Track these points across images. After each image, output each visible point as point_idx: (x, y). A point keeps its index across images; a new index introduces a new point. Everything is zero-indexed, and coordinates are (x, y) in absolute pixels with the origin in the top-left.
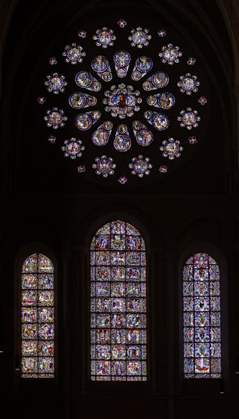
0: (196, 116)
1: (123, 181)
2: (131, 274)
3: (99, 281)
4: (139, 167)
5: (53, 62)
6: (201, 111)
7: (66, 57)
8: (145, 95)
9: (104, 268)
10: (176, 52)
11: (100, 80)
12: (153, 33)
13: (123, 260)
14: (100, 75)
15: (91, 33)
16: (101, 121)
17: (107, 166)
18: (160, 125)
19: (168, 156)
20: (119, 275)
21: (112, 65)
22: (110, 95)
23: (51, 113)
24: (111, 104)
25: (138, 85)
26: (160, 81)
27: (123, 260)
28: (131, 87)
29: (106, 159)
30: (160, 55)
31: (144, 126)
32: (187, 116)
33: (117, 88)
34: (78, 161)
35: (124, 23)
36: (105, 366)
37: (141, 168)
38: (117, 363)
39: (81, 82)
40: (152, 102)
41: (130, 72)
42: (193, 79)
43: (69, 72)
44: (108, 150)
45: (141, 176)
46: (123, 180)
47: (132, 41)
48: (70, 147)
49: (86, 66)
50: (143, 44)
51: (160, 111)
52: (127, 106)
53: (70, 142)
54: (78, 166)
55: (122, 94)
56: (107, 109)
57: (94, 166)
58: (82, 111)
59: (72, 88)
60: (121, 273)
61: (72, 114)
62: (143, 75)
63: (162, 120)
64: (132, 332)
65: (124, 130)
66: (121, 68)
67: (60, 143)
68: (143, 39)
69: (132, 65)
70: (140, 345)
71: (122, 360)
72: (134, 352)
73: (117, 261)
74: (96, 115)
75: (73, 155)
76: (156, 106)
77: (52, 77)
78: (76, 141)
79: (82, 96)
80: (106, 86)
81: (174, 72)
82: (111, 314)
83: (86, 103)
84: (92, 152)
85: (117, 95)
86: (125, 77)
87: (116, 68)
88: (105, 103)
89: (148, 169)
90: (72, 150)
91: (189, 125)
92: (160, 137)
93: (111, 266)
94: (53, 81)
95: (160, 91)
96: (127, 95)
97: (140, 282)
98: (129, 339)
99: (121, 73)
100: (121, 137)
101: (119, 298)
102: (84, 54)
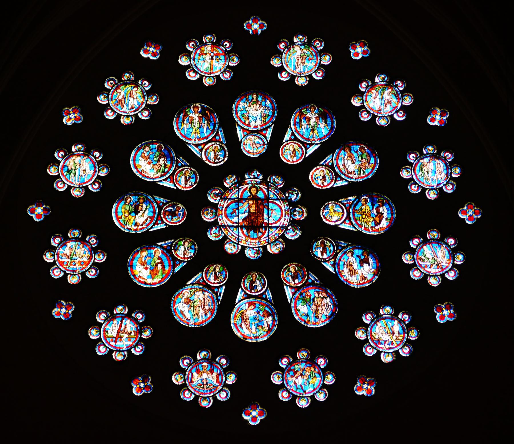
0: (453, 252)
1: (254, 419)
4: (300, 381)
5: (70, 119)
6: (465, 240)
7: (107, 107)
8: (315, 199)
10: (397, 96)
11: (196, 162)
12: (337, 48)
14: (195, 150)
15: (174, 48)
16: (194, 267)
17: (212, 378)
18: (356, 273)
19: (379, 353)
21: (228, 125)
22: (224, 199)
23: (63, 244)
24: (223, 220)
25: (296, 176)
26: (354, 165)
28: (279, 180)
29: (211, 361)
30: (356, 102)
31: (313, 277)
32: (427, 250)
33: (241, 182)
34: (132, 366)
35: (261, 26)
37: (304, 383)
39: (146, 164)
40: (333, 215)
41: (276, 142)
42: (444, 160)
43: (113, 142)
44: (217, 338)
45: (303, 404)
46: (253, 417)
47: (282, 69)
48: (112, 329)
49: (157, 129)
50: (310, 76)
51: (356, 239)
52: (268, 226)
53: (112, 317)
54: (134, 377)
55: (254, 198)
56: (213, 235)
57: (177, 379)
58: (147, 240)
59: (121, 182)
61: (120, 247)
62: (311, 150)
63: (362, 262)
65: (260, 285)
66: (251, 132)
67: (85, 319)
68: (311, 64)
69: (281, 126)
74: (185, 251)
75: (119, 350)
76: (343, 226)
77: (69, 154)
78: (129, 316)
79: (146, 200)
80: (210, 177)
81: (393, 144)
83: (157, 218)
84: (170, 342)
85: (240, 200)
86: (262, 156)
87: (240, 133)
88: (208, 217)
89: (324, 386)
90: (118, 337)
91: (436, 276)
92: (354, 305)
94: (70, 163)
95: (355, 189)
96: (267, 199)
99: (252, 147)
100: (250, 304)
102: (153, 101)
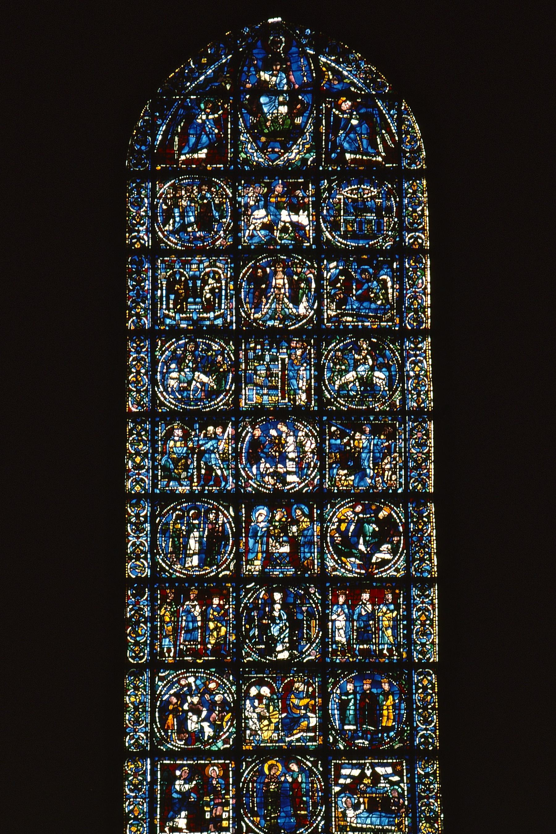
2: (347, 290)
3: (175, 332)
9: (198, 266)
13: (303, 218)
20: (287, 303)
27: (303, 218)
36: (205, 787)
38: (273, 767)
60: (294, 286)
64: (354, 601)
70: (402, 670)
71: (304, 751)
72: (369, 709)
73: (268, 227)
82: (243, 500)
93: (238, 254)
97: (403, 334)
98: (341, 637)
101: (279, 415)
